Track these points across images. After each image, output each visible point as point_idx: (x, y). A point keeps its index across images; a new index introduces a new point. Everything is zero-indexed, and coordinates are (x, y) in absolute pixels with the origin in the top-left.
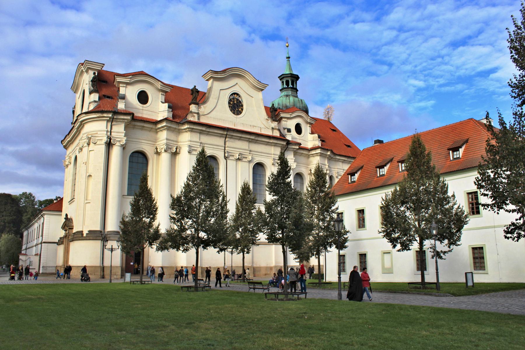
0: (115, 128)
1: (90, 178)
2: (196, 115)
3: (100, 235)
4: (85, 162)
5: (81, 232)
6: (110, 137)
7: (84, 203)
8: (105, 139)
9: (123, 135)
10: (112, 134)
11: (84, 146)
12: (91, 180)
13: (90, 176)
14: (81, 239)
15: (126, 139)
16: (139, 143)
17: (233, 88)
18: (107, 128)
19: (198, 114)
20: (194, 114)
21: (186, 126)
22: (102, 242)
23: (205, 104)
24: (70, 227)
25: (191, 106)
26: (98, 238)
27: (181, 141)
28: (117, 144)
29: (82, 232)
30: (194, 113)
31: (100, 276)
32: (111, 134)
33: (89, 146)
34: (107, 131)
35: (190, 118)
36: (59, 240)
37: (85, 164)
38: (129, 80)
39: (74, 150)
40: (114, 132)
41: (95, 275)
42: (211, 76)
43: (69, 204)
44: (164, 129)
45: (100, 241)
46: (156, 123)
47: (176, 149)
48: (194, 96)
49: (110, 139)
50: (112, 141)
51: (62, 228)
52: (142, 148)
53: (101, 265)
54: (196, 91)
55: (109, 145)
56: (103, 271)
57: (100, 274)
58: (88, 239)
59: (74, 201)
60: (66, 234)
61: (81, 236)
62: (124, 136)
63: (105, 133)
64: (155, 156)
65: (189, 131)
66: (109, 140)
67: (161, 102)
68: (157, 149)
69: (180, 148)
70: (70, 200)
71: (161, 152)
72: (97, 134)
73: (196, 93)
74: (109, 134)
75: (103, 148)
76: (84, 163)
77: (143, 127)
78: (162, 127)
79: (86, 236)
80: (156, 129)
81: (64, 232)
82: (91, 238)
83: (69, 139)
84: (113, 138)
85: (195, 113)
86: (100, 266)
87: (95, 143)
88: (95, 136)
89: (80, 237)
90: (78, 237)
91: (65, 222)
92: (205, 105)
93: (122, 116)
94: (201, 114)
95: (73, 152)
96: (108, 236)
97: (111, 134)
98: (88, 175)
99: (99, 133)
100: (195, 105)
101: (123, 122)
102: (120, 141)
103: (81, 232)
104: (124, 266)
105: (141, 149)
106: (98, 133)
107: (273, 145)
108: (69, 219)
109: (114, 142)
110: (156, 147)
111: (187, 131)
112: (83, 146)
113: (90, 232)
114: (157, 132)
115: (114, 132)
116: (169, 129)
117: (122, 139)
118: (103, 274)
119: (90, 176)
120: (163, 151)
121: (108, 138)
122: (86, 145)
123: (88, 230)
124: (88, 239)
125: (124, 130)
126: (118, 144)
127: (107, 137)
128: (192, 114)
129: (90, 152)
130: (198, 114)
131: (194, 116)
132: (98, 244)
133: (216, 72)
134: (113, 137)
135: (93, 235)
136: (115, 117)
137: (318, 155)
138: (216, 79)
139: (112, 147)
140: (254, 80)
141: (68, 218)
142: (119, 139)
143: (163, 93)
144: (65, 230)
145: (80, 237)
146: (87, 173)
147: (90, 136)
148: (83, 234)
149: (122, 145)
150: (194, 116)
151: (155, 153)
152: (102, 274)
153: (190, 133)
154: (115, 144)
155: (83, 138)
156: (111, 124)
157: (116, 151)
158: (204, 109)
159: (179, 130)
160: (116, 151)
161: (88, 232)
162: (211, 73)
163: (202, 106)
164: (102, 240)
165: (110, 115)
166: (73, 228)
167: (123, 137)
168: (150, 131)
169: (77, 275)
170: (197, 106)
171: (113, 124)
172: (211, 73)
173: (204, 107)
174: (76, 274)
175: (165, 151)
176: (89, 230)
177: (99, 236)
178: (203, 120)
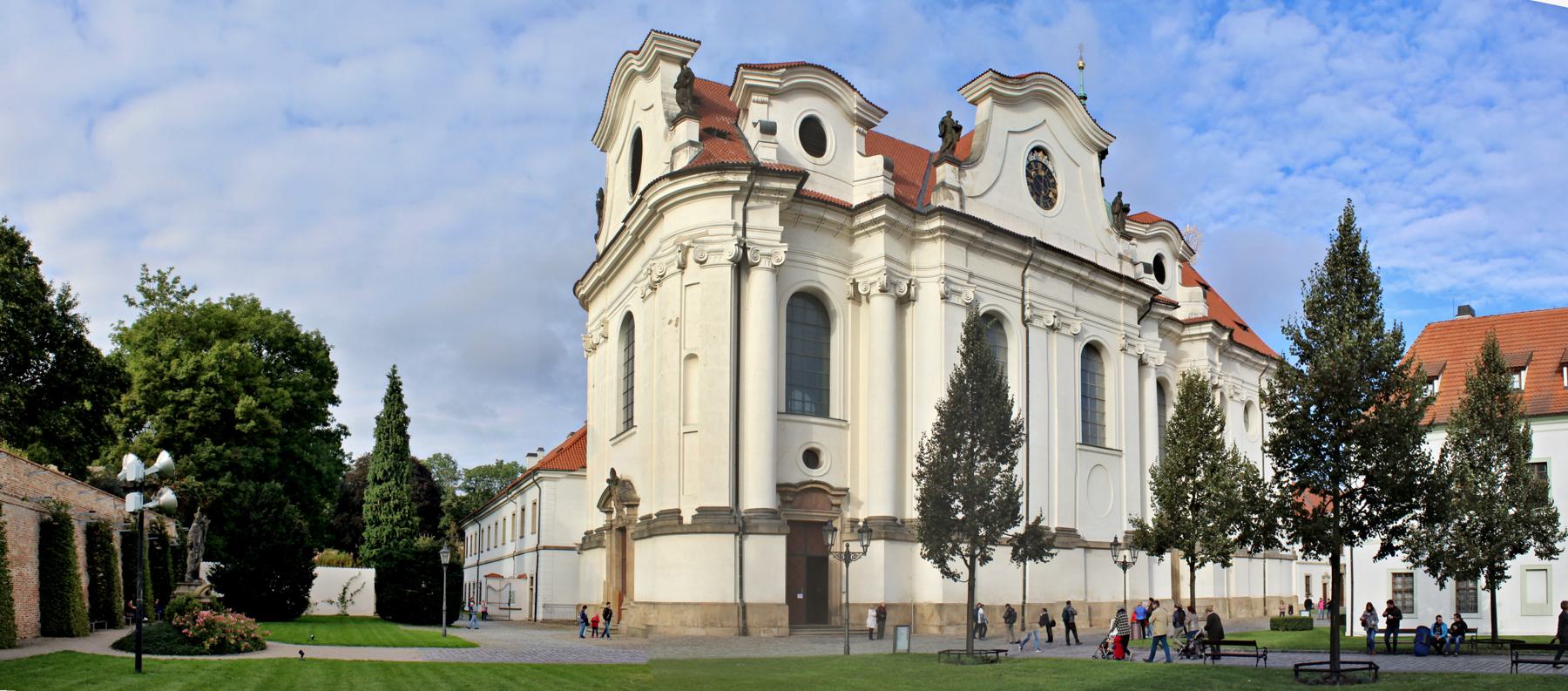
0: (754, 219)
1: (692, 362)
2: (955, 194)
3: (733, 521)
4: (674, 319)
5: (676, 513)
6: (745, 244)
7: (679, 434)
8: (731, 249)
9: (778, 237)
10: (749, 234)
12: (696, 369)
13: (692, 357)
14: (678, 531)
15: (786, 250)
16: (814, 268)
17: (1037, 130)
18: (733, 218)
19: (960, 191)
20: (951, 191)
22: (738, 537)
23: (975, 166)
24: (631, 503)
25: (939, 169)
26: (727, 528)
29: (679, 511)
30: (950, 188)
31: (736, 630)
33: (683, 273)
34: (735, 227)
35: (939, 200)
36: (584, 539)
37: (676, 325)
39: (620, 300)
40: (753, 229)
41: (722, 627)
43: (613, 445)
44: (879, 228)
46: (853, 211)
48: (949, 141)
49: (745, 249)
50: (749, 253)
51: (598, 506)
53: (738, 601)
55: (741, 266)
56: (744, 617)
57: (736, 624)
58: (699, 530)
59: (635, 433)
60: (611, 521)
61: (676, 522)
62: (781, 242)
63: (731, 230)
66: (741, 251)
70: (615, 435)
72: (707, 234)
74: (740, 233)
75: (727, 273)
76: (670, 322)
77: (822, 220)
78: (875, 221)
79: (693, 524)
80: (852, 231)
81: (604, 516)
82: (708, 528)
83: (600, 274)
84: (751, 247)
85: (953, 188)
86: (736, 604)
87: (701, 263)
88: (703, 242)
89: (675, 526)
90: (669, 526)
91: (609, 488)
92: (974, 170)
94: (966, 192)
95: (616, 305)
96: (753, 521)
98: (685, 353)
99: (712, 231)
100: (952, 167)
102: (770, 255)
103: (676, 513)
106: (710, 233)
108: (624, 482)
109: (755, 258)
112: (662, 276)
113: (703, 511)
114: (852, 240)
115: (753, 229)
116: (890, 227)
117: (777, 249)
118: (745, 624)
119: (692, 357)
122: (674, 269)
124: (699, 530)
125: (780, 225)
126: (764, 263)
127: (736, 242)
128: (946, 191)
129: (688, 288)
130: (960, 191)
131: (951, 198)
132: (727, 542)
134: (752, 243)
139: (748, 273)
141: (618, 479)
142: (767, 251)
144: (606, 512)
145: (675, 526)
146: (683, 351)
147: (686, 243)
148: (681, 519)
149: (775, 266)
150: (951, 198)
152: (741, 625)
154: (757, 264)
155: (659, 254)
157: (759, 285)
158: (974, 180)
160: (759, 285)
161: (696, 513)
163: (967, 172)
164: (736, 534)
166: (637, 505)
167: (778, 243)
168: (836, 234)
169: (672, 626)
170: (957, 169)
171: (748, 205)
173: (972, 174)
174: (668, 624)
176: (699, 508)
177: (730, 523)
178: (972, 209)
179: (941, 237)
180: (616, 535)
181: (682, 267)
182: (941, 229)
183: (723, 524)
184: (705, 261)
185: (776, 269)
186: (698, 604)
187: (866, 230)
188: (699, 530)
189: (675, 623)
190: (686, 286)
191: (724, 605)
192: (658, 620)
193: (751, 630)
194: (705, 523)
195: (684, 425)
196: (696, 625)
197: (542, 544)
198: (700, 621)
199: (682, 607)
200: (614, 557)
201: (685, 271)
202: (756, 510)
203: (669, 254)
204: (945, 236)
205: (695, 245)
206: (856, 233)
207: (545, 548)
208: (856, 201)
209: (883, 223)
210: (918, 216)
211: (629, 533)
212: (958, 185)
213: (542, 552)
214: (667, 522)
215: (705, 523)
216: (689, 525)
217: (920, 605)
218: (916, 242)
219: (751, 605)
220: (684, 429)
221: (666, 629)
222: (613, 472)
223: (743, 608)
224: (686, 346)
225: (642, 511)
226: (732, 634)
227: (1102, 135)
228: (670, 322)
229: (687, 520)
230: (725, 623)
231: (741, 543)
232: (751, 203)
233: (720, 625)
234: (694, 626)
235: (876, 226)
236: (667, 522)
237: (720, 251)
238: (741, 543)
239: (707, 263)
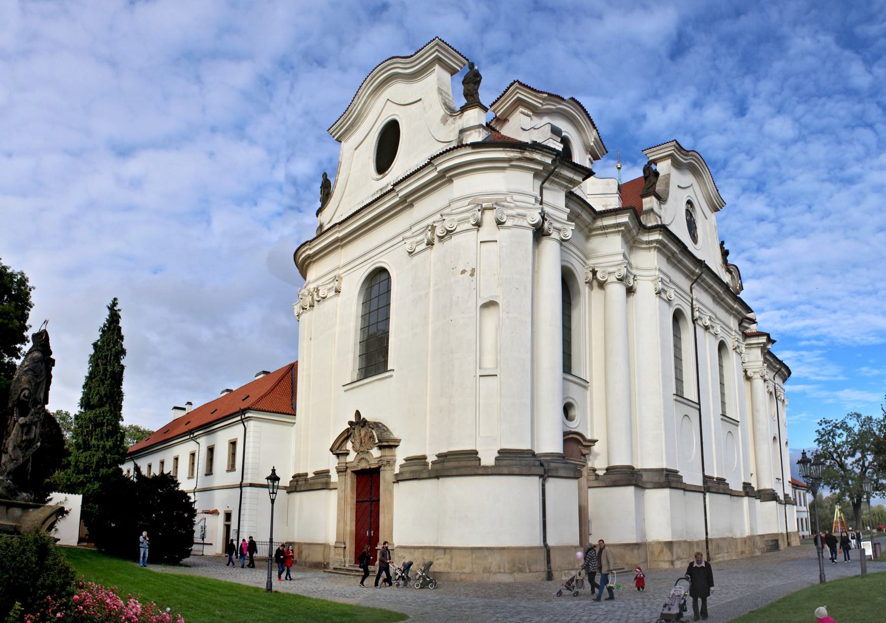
0: (548, 196)
1: (490, 313)
5: (473, 454)
11: (457, 230)
15: (573, 228)
16: (569, 252)
22: (541, 480)
27: (640, 266)
33: (478, 231)
41: (530, 571)
42: (673, 152)
45: (537, 478)
50: (546, 224)
52: (572, 264)
58: (506, 471)
59: (391, 376)
68: (594, 272)
71: (606, 280)
75: (530, 234)
79: (495, 466)
80: (591, 230)
82: (516, 470)
84: (548, 219)
88: (503, 206)
91: (348, 430)
93: (568, 171)
98: (481, 302)
105: (570, 266)
107: (734, 314)
111: (652, 247)
113: (504, 454)
117: (566, 227)
118: (549, 567)
120: (612, 278)
123: (437, 453)
124: (506, 471)
126: (555, 235)
129: (482, 244)
133: (680, 148)
135: (518, 462)
137: (758, 347)
138: (677, 164)
140: (713, 188)
153: (656, 252)
162: (674, 146)
164: (541, 476)
165: (549, 161)
169: (472, 573)
171: (544, 185)
172: (674, 146)
174: (467, 570)
175: (620, 280)
176: (501, 450)
177: (534, 466)
179: (655, 248)
180: (352, 478)
181: (478, 225)
182: (657, 241)
183: (530, 466)
185: (562, 242)
186: (504, 548)
187: (606, 231)
188: (506, 471)
189: (476, 571)
191: (531, 549)
192: (450, 566)
193: (556, 574)
194: (511, 465)
196: (502, 570)
197: (247, 480)
198: (507, 566)
199: (486, 553)
200: (349, 499)
201: (481, 229)
202: (552, 454)
203: (462, 212)
204: (658, 248)
205: (497, 208)
206: (594, 233)
207: (251, 485)
210: (642, 229)
211: (386, 476)
213: (247, 491)
214: (463, 463)
215: (511, 465)
216: (492, 467)
218: (634, 249)
219: (554, 548)
220: (479, 373)
221: (463, 577)
222: (358, 414)
223: (547, 549)
224: (481, 296)
225: (400, 455)
226: (540, 579)
227: (720, 202)
228: (463, 272)
229: (488, 459)
230: (533, 568)
231: (543, 485)
232: (546, 185)
233: (528, 571)
234: (500, 573)
235: (617, 229)
236: (463, 463)
237: (523, 216)
238: (543, 485)
239: (506, 225)
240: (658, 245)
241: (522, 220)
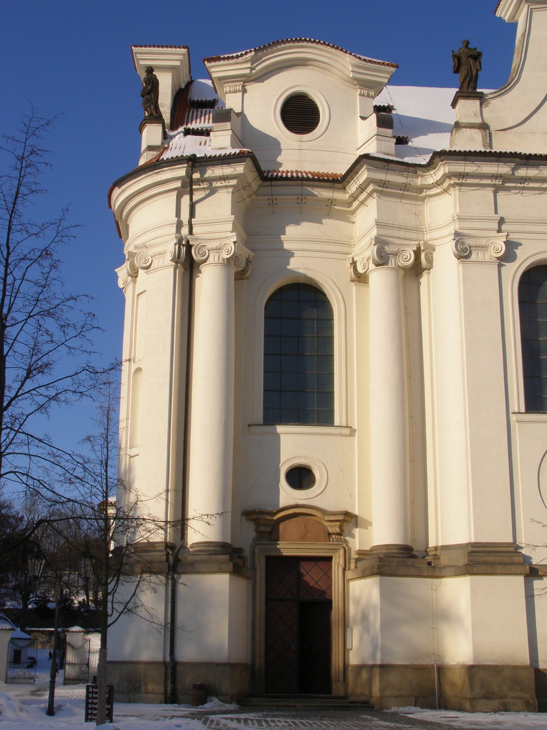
6: (188, 242)
10: (195, 230)
21: (442, 170)
28: (211, 260)
32: (191, 232)
38: (249, 65)
44: (370, 195)
47: (417, 253)
49: (189, 247)
53: (168, 659)
54: (470, 56)
56: (174, 682)
57: (162, 690)
62: (232, 232)
64: (354, 287)
65: (454, 185)
66: (184, 249)
67: (361, 117)
68: (354, 264)
69: (427, 251)
73: (471, 61)
74: (185, 231)
78: (362, 188)
84: (196, 243)
86: (164, 663)
87: (149, 267)
97: (191, 232)
101: (226, 187)
102: (218, 249)
104: (260, 662)
110: (353, 259)
121: (179, 243)
126: (213, 258)
127: (175, 241)
130: (484, 127)
134: (197, 239)
136: (196, 176)
143: (366, 92)
151: (352, 281)
156: (191, 199)
159: (420, 189)
184: (149, 267)
190: (139, 295)
195: (130, 448)
208: (342, 170)
209: (371, 188)
212: (478, 120)
217: (451, 668)
219: (184, 664)
240: (452, 182)
241: (162, 260)
